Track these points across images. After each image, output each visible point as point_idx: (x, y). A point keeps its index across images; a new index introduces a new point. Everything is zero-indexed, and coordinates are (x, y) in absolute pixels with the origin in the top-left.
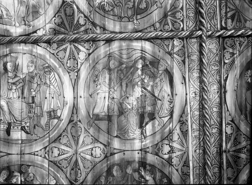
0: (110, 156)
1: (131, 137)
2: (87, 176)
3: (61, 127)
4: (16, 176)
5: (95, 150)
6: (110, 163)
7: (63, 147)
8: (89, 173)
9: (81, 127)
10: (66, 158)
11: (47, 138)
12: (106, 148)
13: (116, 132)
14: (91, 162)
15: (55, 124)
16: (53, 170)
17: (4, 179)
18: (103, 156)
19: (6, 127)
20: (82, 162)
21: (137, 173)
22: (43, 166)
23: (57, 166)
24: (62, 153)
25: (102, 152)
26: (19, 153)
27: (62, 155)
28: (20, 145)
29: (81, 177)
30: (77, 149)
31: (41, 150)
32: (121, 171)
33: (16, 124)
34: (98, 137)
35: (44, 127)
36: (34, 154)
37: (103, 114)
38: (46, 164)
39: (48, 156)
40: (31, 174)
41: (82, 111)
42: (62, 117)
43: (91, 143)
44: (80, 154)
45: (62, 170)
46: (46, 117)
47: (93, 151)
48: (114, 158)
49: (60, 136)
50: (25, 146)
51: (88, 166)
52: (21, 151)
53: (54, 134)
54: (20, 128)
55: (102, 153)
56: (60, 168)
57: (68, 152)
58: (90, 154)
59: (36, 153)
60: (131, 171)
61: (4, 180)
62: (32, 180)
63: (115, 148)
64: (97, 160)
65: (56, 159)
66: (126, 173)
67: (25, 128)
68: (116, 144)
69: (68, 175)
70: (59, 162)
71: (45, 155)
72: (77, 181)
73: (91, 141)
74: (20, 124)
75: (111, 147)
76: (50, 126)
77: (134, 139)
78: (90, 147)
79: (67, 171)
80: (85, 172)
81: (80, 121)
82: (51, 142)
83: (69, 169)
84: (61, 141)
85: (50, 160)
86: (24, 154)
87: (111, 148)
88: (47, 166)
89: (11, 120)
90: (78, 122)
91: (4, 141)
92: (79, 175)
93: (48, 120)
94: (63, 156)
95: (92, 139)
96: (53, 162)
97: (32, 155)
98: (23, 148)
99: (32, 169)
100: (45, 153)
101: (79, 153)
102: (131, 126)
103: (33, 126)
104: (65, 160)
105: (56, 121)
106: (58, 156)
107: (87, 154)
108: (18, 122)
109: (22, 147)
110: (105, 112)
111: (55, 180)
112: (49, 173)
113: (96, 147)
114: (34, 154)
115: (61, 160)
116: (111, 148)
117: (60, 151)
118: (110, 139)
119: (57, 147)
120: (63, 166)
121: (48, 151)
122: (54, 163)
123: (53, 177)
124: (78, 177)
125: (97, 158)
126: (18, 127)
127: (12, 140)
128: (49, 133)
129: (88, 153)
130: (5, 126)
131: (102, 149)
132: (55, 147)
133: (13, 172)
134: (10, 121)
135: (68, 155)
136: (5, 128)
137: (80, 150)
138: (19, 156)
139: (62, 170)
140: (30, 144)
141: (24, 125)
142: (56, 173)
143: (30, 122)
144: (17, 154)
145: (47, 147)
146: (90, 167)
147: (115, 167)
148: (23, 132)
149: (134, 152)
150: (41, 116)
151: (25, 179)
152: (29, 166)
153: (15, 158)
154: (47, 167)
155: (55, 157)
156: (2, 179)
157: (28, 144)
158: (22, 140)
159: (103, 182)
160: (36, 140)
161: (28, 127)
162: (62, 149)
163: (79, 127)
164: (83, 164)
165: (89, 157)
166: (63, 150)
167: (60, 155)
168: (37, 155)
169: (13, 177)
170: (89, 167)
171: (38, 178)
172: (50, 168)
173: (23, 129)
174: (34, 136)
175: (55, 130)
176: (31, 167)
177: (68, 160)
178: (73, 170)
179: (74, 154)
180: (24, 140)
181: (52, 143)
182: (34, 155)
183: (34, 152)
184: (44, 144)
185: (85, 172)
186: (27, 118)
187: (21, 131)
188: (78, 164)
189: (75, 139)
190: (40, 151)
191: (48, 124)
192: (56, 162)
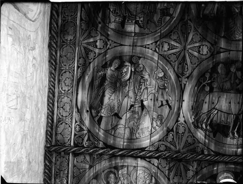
0: (216, 54)
1: (237, 38)
2: (193, 71)
3: (172, 24)
4: (127, 66)
5: (203, 48)
6: (216, 61)
7: (173, 43)
8: (195, 69)
9: (191, 26)
10: (175, 53)
11: (158, 33)
12: (213, 47)
13: (223, 32)
14: (198, 59)
15: (167, 20)
16: (162, 63)
17: (115, 68)
18: (209, 54)
19: (121, 20)
20: (190, 58)
21: (240, 72)
22: (153, 59)
23: (166, 59)
24: (171, 48)
25: (208, 50)
26: (132, 45)
27: (171, 50)
28: (132, 38)
29: (187, 71)
30: (186, 45)
31: (152, 44)
32: (225, 69)
33: (131, 18)
34: (206, 36)
35: (157, 22)
36: (146, 46)
37: (212, 15)
38: (156, 57)
39: (159, 50)
40: (140, 65)
41: (193, 11)
42: (174, 15)
43: (199, 41)
44: (188, 50)
45: (171, 64)
46: (159, 13)
47: (200, 49)
48: (220, 56)
49: (171, 32)
50: (137, 39)
51: (195, 62)
52: (133, 44)
53: (165, 30)
54: (134, 22)
55: (208, 51)
56: (169, 62)
57: (177, 47)
58: (198, 51)
59: (147, 46)
60: (235, 70)
61: (115, 69)
62: (142, 71)
63: (221, 47)
64: (204, 57)
65: (165, 53)
66: (230, 71)
67: (139, 22)
68: (223, 44)
69: (176, 69)
70: (168, 56)
71: (155, 49)
72: (184, 75)
73: (200, 39)
74: (135, 19)
75: (218, 46)
76: (163, 22)
77: (239, 40)
78: (197, 45)
79: (175, 65)
80: (192, 67)
81: (190, 20)
82: (162, 37)
83: (176, 63)
84: (172, 37)
85: (160, 53)
86: (136, 46)
87: (217, 47)
88: (157, 59)
89: (126, 14)
90: (188, 20)
91: (117, 33)
92: (186, 70)
93: (161, 16)
94: (172, 51)
95: (200, 37)
96: (163, 56)
97: (143, 48)
98: (136, 41)
99: (142, 61)
100: (156, 47)
101: (187, 49)
102: (238, 28)
103: (146, 22)
104: (174, 54)
105: (168, 18)
106: (168, 51)
107: (195, 51)
108: (132, 16)
109: (135, 39)
110: (214, 14)
111: (163, 73)
112: (158, 65)
113: (203, 45)
114: (146, 47)
115: (171, 54)
116: (217, 47)
117: (170, 46)
118: (217, 39)
119: (167, 43)
120: (172, 61)
121: (159, 45)
122: (163, 57)
123: (162, 70)
124: (185, 72)
125: (204, 55)
126: (132, 21)
127: (126, 32)
128: (161, 28)
129: (195, 50)
130: (121, 19)
131: (209, 48)
132: (166, 42)
133: (125, 62)
134: (125, 15)
135: (177, 50)
136: (120, 21)
137: (189, 47)
138: (131, 47)
139: (171, 64)
140: (142, 37)
141: (138, 19)
142: (164, 65)
143: (144, 17)
144: (130, 46)
145: (158, 41)
146: (197, 63)
147: (220, 65)
148: (137, 26)
149: (239, 52)
150: (155, 13)
151: (135, 69)
152: (140, 58)
153: (127, 50)
154: (157, 59)
155: (165, 51)
156: (114, 68)
157: (140, 37)
158: (136, 33)
159: (208, 78)
160: (149, 34)
161: (141, 21)
162: (171, 44)
163: (189, 25)
164: (190, 60)
165: (196, 54)
166: (173, 45)
167: (170, 50)
168: (148, 48)
169: (124, 67)
170: (195, 63)
171: (147, 69)
172: (159, 61)
173: (137, 23)
174: (147, 30)
175: (167, 27)
176: (141, 59)
177: (177, 55)
178: (181, 64)
179: (182, 50)
180: (137, 33)
181: (163, 38)
182: (145, 48)
183: (146, 45)
184: (155, 38)
185: (192, 67)
186: (141, 13)
187: (135, 25)
188: (186, 59)
189: (185, 36)
190: (151, 45)
191: (160, 21)
192: (165, 56)
